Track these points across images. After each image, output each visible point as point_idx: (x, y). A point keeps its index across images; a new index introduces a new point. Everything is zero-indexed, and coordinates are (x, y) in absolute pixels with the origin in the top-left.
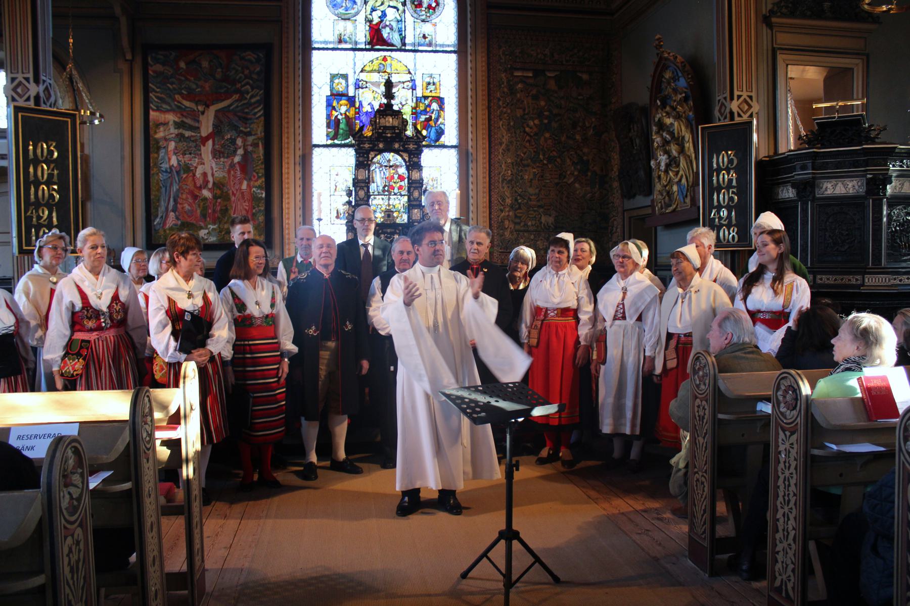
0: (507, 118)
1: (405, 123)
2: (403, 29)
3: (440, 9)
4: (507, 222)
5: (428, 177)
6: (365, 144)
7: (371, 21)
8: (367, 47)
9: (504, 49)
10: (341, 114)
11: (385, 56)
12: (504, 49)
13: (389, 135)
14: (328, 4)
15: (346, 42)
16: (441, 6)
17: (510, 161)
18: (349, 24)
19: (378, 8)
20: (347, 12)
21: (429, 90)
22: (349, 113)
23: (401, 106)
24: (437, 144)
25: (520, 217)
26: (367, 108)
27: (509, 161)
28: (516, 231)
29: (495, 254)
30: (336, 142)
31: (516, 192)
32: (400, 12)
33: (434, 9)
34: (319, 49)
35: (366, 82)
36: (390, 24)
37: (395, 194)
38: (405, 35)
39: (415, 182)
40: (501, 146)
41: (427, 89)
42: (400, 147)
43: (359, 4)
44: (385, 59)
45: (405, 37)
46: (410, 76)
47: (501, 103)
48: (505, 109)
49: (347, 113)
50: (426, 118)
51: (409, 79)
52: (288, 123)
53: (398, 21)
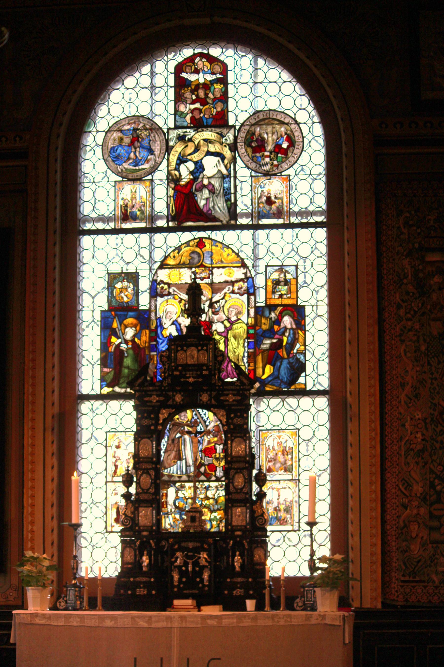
0: (415, 338)
1: (220, 358)
2: (233, 191)
3: (296, 151)
4: (414, 528)
5: (276, 448)
6: (151, 396)
8: (171, 224)
9: (408, 215)
10: (126, 342)
11: (201, 239)
12: (408, 215)
13: (191, 380)
14: (106, 156)
15: (135, 218)
16: (298, 146)
17: (420, 416)
19: (189, 157)
20: (137, 168)
21: (277, 296)
22: (139, 339)
23: (228, 325)
24: (293, 388)
25: (439, 518)
27: (418, 415)
28: (432, 543)
29: (393, 585)
31: (432, 472)
32: (226, 161)
33: (285, 152)
34: (90, 232)
35: (169, 285)
36: (210, 183)
38: (236, 201)
39: (239, 459)
40: (403, 390)
41: (274, 292)
42: (210, 400)
43: (157, 152)
44: (201, 243)
45: (235, 204)
46: (245, 271)
47: (402, 312)
48: (410, 323)
49: (136, 340)
50: (272, 344)
51: (243, 276)
52: (34, 360)
53: (223, 177)
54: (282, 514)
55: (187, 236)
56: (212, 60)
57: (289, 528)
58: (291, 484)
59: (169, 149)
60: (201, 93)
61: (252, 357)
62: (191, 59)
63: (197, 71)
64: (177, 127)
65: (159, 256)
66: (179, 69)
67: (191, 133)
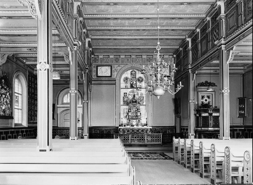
18: (127, 84)
26: (130, 99)
44: (133, 90)
55: (132, 89)
56: (134, 71)
62: (132, 71)
66: (131, 72)
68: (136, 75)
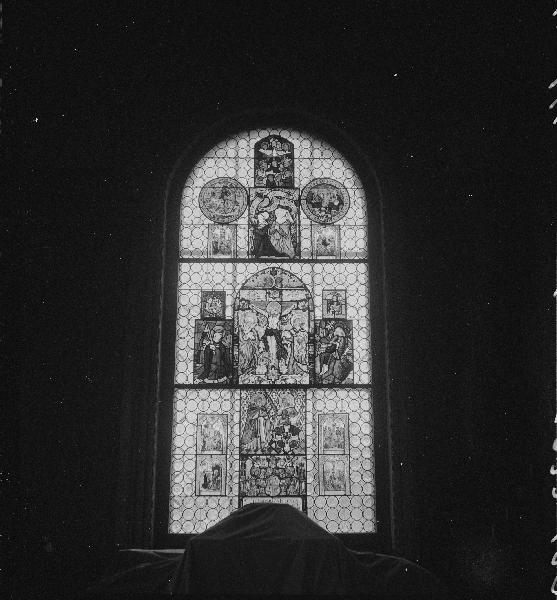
7: (255, 226)
11: (273, 268)
18: (228, 231)
30: (207, 381)
33: (337, 208)
34: (188, 261)
37: (286, 454)
38: (300, 243)
44: (274, 272)
54: (337, 482)
55: (262, 266)
56: (283, 141)
57: (342, 493)
58: (344, 458)
59: (249, 203)
60: (275, 164)
61: (312, 358)
62: (266, 140)
63: (271, 148)
64: (255, 187)
65: (241, 279)
66: (258, 146)
67: (266, 192)
68: (291, 168)
